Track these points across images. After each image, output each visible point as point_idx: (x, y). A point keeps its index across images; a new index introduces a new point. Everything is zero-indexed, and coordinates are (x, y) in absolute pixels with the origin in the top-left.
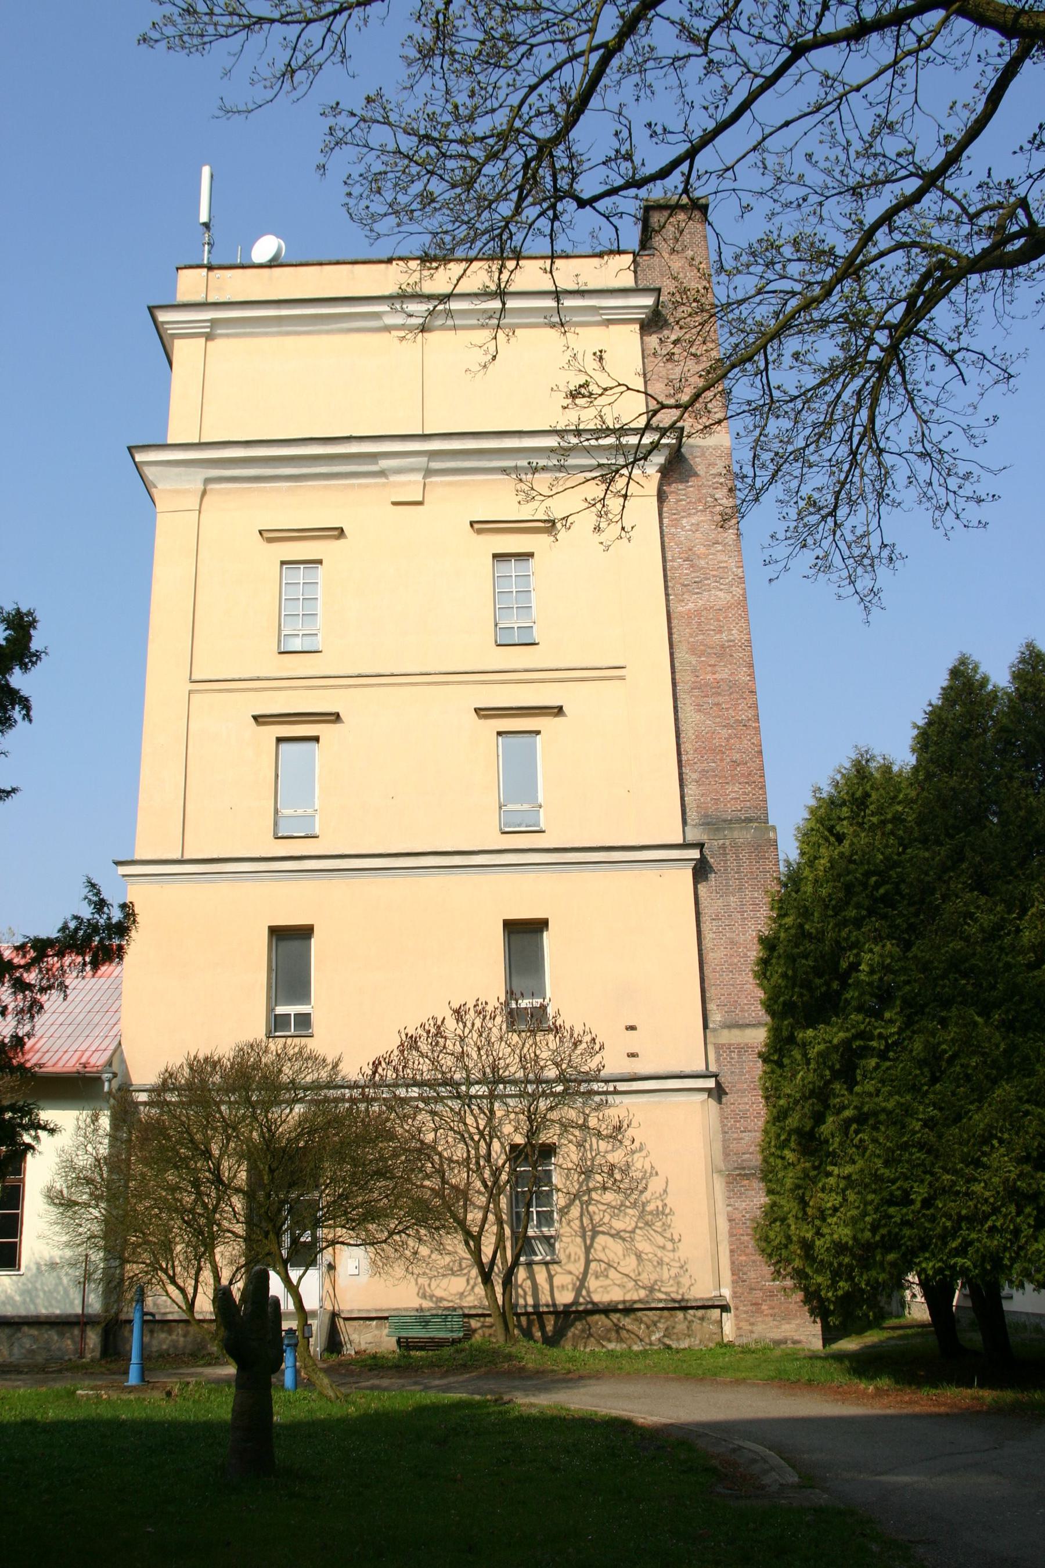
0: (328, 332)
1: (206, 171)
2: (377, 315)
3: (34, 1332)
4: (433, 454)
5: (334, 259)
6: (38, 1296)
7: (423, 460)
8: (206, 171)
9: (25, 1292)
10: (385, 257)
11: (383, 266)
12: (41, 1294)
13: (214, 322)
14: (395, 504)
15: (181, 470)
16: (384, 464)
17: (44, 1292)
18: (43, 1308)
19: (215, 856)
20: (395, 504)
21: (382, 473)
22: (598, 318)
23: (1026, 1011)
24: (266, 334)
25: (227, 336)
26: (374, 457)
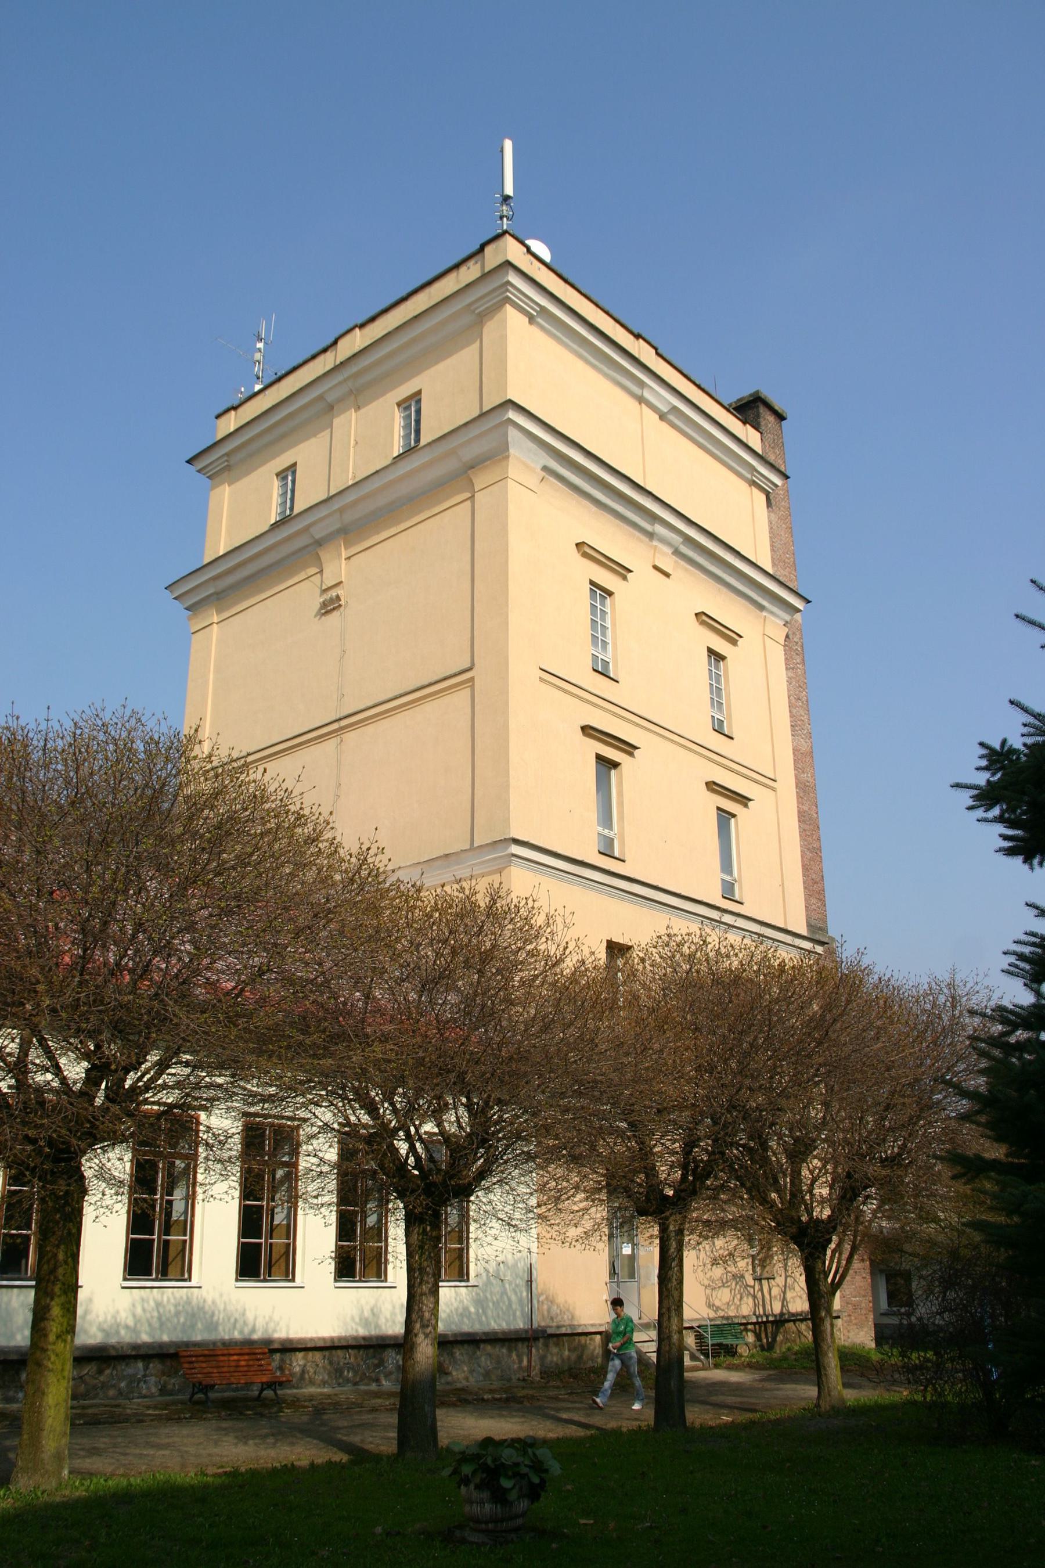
0: (606, 376)
1: (508, 145)
2: (642, 384)
3: (489, 1348)
4: (688, 540)
5: (607, 308)
6: (488, 1306)
7: (677, 539)
8: (508, 145)
9: (479, 1302)
10: (636, 332)
11: (631, 337)
12: (491, 1305)
13: (543, 310)
14: (656, 567)
15: (532, 446)
16: (659, 529)
17: (493, 1303)
18: (497, 1324)
19: (655, 884)
20: (656, 567)
21: (651, 535)
22: (749, 476)
23: (206, 907)
24: (566, 346)
25: (542, 328)
26: (654, 518)
